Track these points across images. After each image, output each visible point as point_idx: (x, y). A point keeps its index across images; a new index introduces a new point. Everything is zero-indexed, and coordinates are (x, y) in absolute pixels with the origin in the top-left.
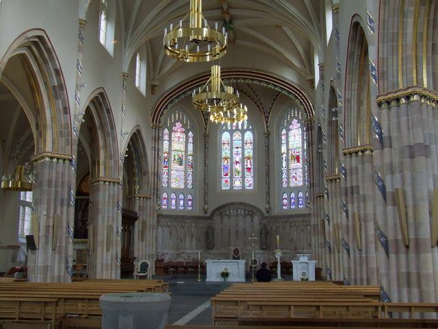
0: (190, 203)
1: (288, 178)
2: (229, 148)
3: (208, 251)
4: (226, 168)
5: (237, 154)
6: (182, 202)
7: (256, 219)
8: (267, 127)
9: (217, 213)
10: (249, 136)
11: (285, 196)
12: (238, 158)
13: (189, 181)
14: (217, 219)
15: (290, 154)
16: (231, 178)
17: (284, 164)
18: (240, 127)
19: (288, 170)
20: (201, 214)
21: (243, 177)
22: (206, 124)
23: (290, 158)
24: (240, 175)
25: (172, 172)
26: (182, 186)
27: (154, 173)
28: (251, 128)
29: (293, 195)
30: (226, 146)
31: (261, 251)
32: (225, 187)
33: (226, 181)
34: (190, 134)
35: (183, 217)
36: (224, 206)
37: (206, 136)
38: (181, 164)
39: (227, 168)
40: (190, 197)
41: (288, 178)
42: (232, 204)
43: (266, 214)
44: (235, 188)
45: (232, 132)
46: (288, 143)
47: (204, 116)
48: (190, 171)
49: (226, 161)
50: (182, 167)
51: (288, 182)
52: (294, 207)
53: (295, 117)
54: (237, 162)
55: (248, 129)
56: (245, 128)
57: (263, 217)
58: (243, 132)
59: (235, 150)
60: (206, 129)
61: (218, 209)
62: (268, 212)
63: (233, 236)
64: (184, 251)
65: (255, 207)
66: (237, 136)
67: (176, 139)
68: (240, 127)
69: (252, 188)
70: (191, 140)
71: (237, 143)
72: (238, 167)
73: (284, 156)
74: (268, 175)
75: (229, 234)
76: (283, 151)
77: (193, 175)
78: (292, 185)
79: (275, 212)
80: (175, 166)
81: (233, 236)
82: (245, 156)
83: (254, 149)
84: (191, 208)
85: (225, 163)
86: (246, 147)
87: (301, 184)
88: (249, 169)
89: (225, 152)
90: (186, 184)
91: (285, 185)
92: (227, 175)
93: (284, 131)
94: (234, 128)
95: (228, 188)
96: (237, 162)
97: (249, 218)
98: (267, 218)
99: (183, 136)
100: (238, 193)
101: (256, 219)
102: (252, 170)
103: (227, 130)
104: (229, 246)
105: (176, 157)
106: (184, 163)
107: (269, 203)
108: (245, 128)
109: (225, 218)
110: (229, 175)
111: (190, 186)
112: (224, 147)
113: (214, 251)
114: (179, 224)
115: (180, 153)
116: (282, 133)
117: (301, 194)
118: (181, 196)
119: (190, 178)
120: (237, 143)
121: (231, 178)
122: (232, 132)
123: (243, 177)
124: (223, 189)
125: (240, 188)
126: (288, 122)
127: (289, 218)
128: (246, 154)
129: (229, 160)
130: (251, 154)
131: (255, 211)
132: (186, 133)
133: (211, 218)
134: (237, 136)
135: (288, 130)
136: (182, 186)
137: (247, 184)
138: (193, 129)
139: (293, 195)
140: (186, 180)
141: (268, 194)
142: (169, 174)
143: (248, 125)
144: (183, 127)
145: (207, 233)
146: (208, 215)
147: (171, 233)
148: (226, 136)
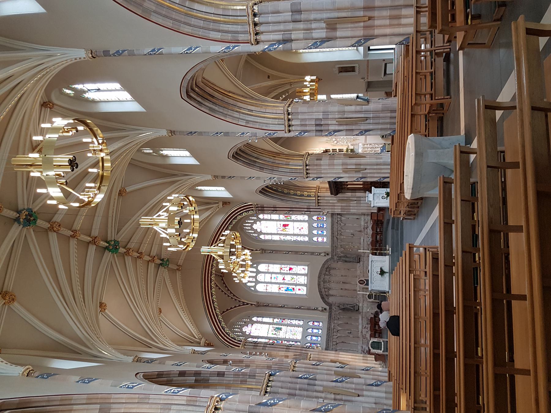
0: (316, 324)
1: (301, 235)
2: (270, 285)
3: (360, 310)
4: (287, 289)
5: (277, 278)
6: (315, 331)
7: (334, 265)
8: (256, 250)
9: (326, 299)
10: (262, 267)
11: (315, 239)
12: (280, 278)
13: (297, 324)
14: (331, 300)
15: (279, 232)
16: (296, 285)
17: (288, 238)
18: (254, 275)
19: (294, 235)
20: (325, 316)
21: (297, 274)
22: (248, 304)
23: (284, 233)
24: (295, 277)
25: (287, 337)
26: (301, 329)
27: (286, 349)
28: (255, 265)
29: (315, 232)
30: (268, 288)
31: (361, 263)
32: (303, 291)
33: (299, 290)
34: (255, 319)
35: (329, 329)
36: (320, 292)
37: (258, 305)
38: (280, 329)
39: (288, 288)
40: (311, 324)
41: (301, 235)
42: (319, 285)
43: (330, 257)
44: (306, 283)
45: (257, 282)
46: (271, 234)
47: (239, 306)
48: (287, 321)
49: (282, 289)
50: (284, 328)
51: (304, 235)
52: (325, 232)
53: (251, 226)
54: (284, 279)
55: (256, 268)
56: (254, 270)
57: (332, 258)
58: (258, 272)
59: (273, 281)
60: (252, 305)
61: (323, 298)
62: (328, 254)
63: (347, 286)
64: (360, 331)
65: (324, 264)
66: (260, 277)
67: (257, 331)
68: (254, 275)
69: (306, 268)
70: (260, 319)
71: (267, 278)
72: (288, 278)
73: (282, 238)
74: (296, 253)
75: (346, 289)
76: (279, 239)
77: (291, 320)
78: (306, 232)
79: (328, 248)
80: (281, 335)
81: (347, 286)
82: (279, 272)
83: (274, 263)
84: (321, 323)
85: (283, 291)
86: (272, 271)
87: (306, 225)
88: (291, 269)
89: (274, 289)
90: (298, 326)
91: (306, 239)
92: (293, 289)
93: (262, 237)
94: (254, 280)
95: (305, 288)
96: (284, 279)
97: (332, 272)
98: (332, 255)
99: (255, 325)
100: (310, 281)
101: (334, 265)
102: (291, 266)
103: (255, 287)
104: (356, 290)
105: (274, 332)
106: (280, 327)
107: (320, 253)
108: (254, 270)
109: (331, 292)
110: (294, 287)
111: (301, 323)
112: (269, 290)
113: (361, 305)
114: (335, 334)
115: (270, 330)
116: (263, 238)
117: (315, 225)
118: (310, 331)
119: (294, 322)
120: (267, 278)
121: (296, 285)
122: (257, 282)
123: (297, 274)
124: (305, 293)
125: (306, 277)
126: (254, 233)
127: (334, 236)
128: (278, 271)
129: (281, 286)
130: (279, 266)
131: (326, 266)
132: (253, 323)
133: (330, 305)
134: (260, 277)
135: (261, 233)
136: (301, 329)
137: (303, 272)
138: (250, 317)
139: (315, 232)
140: (295, 326)
141: (312, 253)
142: (288, 340)
143: (254, 267)
144: (247, 326)
145: (344, 309)
146: (328, 307)
147: (342, 342)
148: (260, 288)
